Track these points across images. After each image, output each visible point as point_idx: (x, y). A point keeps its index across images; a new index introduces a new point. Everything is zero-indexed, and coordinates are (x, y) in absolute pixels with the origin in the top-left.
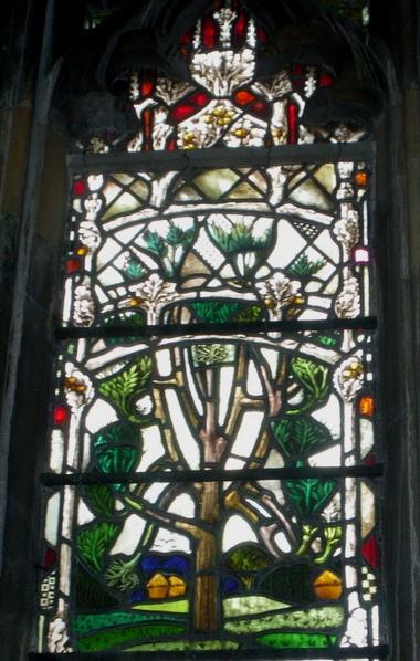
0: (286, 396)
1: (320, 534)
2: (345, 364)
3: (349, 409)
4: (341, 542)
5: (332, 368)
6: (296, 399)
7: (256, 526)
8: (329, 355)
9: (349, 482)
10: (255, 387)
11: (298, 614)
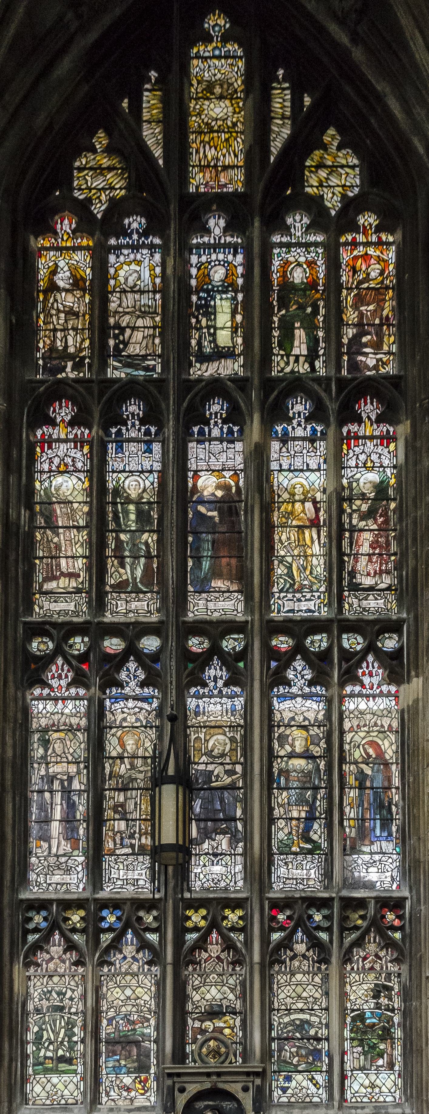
7: (64, 1051)
8: (76, 1018)
10: (63, 1024)
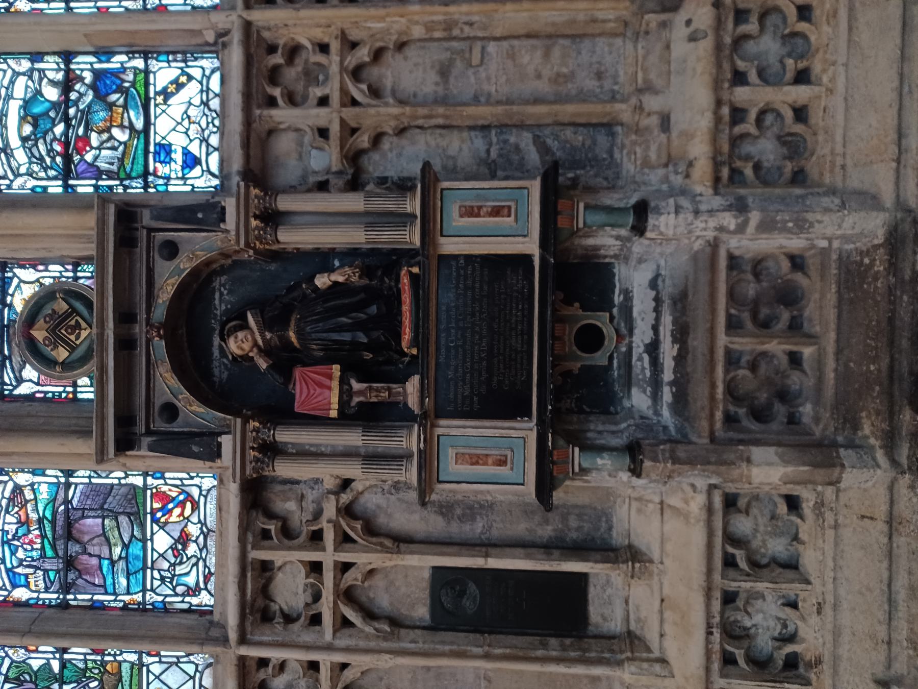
0: (26, 681)
1: (90, 670)
2: (11, 655)
3: (33, 655)
4: (95, 661)
5: (13, 661)
6: (28, 678)
9: (66, 656)
11: (124, 680)
